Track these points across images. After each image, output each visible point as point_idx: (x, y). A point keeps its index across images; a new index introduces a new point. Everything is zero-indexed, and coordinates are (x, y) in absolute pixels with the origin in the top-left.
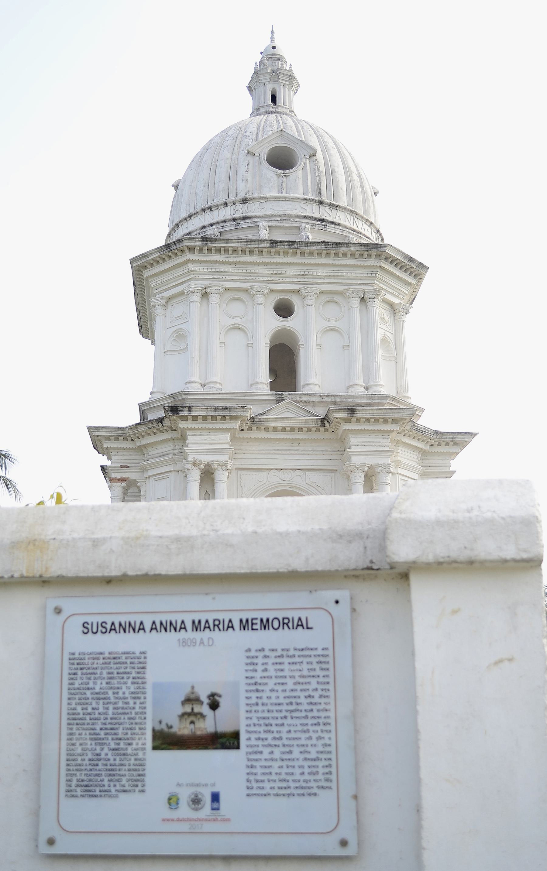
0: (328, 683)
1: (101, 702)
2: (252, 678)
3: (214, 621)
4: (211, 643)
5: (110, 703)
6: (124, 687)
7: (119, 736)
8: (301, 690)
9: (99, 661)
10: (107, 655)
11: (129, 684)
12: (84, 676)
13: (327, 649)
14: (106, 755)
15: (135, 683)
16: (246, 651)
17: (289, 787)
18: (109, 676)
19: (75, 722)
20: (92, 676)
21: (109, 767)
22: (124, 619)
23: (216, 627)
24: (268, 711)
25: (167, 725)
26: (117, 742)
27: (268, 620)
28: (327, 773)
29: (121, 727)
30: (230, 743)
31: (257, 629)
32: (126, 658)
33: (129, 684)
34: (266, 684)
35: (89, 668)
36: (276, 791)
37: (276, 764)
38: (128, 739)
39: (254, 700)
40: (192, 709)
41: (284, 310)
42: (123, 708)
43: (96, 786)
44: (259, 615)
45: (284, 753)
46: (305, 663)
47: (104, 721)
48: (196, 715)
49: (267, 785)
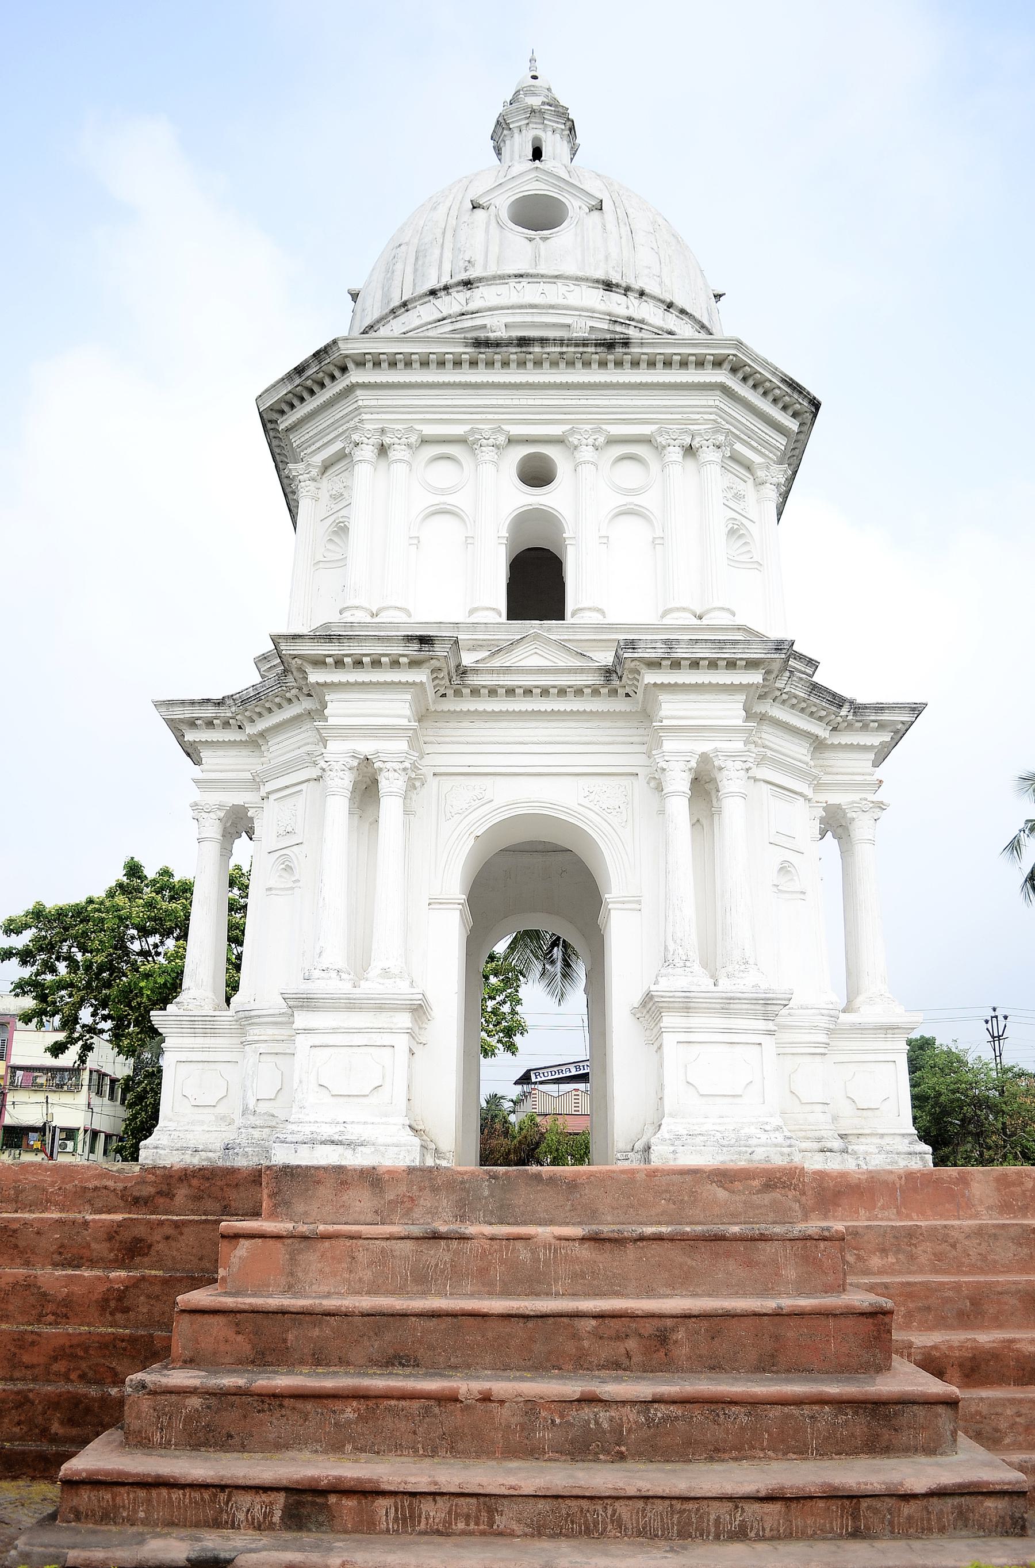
41: (537, 475)
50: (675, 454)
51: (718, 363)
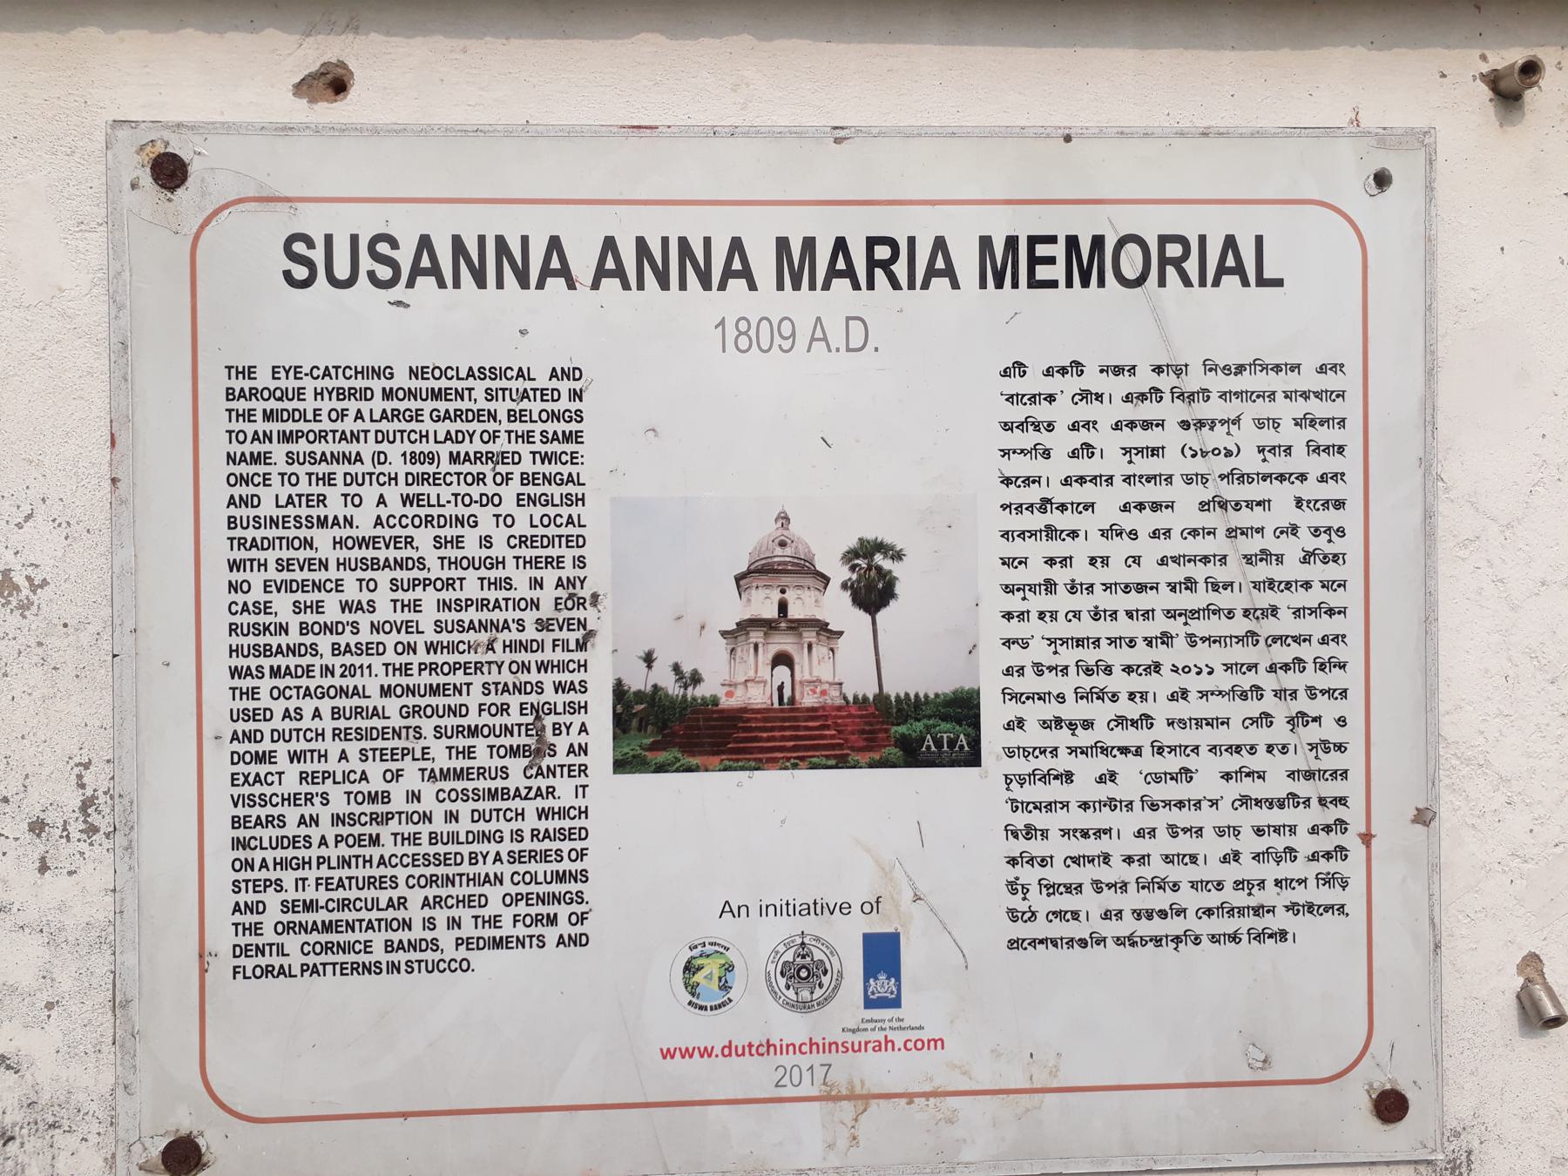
0: (1339, 504)
1: (384, 577)
2: (1029, 481)
3: (872, 242)
4: (856, 342)
5: (426, 583)
6: (485, 515)
7: (473, 719)
8: (1231, 533)
9: (365, 407)
10: (402, 380)
11: (509, 506)
12: (301, 470)
13: (1337, 367)
14: (415, 796)
15: (532, 500)
16: (1006, 373)
17: (1181, 912)
18: (417, 469)
19: (266, 663)
20: (340, 470)
21: (425, 848)
22: (473, 225)
23: (879, 273)
24: (1096, 615)
25: (676, 668)
26: (461, 742)
27: (1098, 242)
28: (1328, 855)
29: (477, 680)
30: (938, 743)
31: (1053, 284)
32: (490, 395)
33: (509, 506)
34: (1090, 506)
35: (322, 436)
36: (1127, 926)
37: (1125, 822)
38: (508, 730)
39: (1036, 572)
40: (783, 607)
42: (483, 604)
43: (370, 926)
44: (1060, 223)
45: (1157, 778)
46: (1246, 422)
47: (398, 660)
48: (797, 626)
49: (1088, 902)
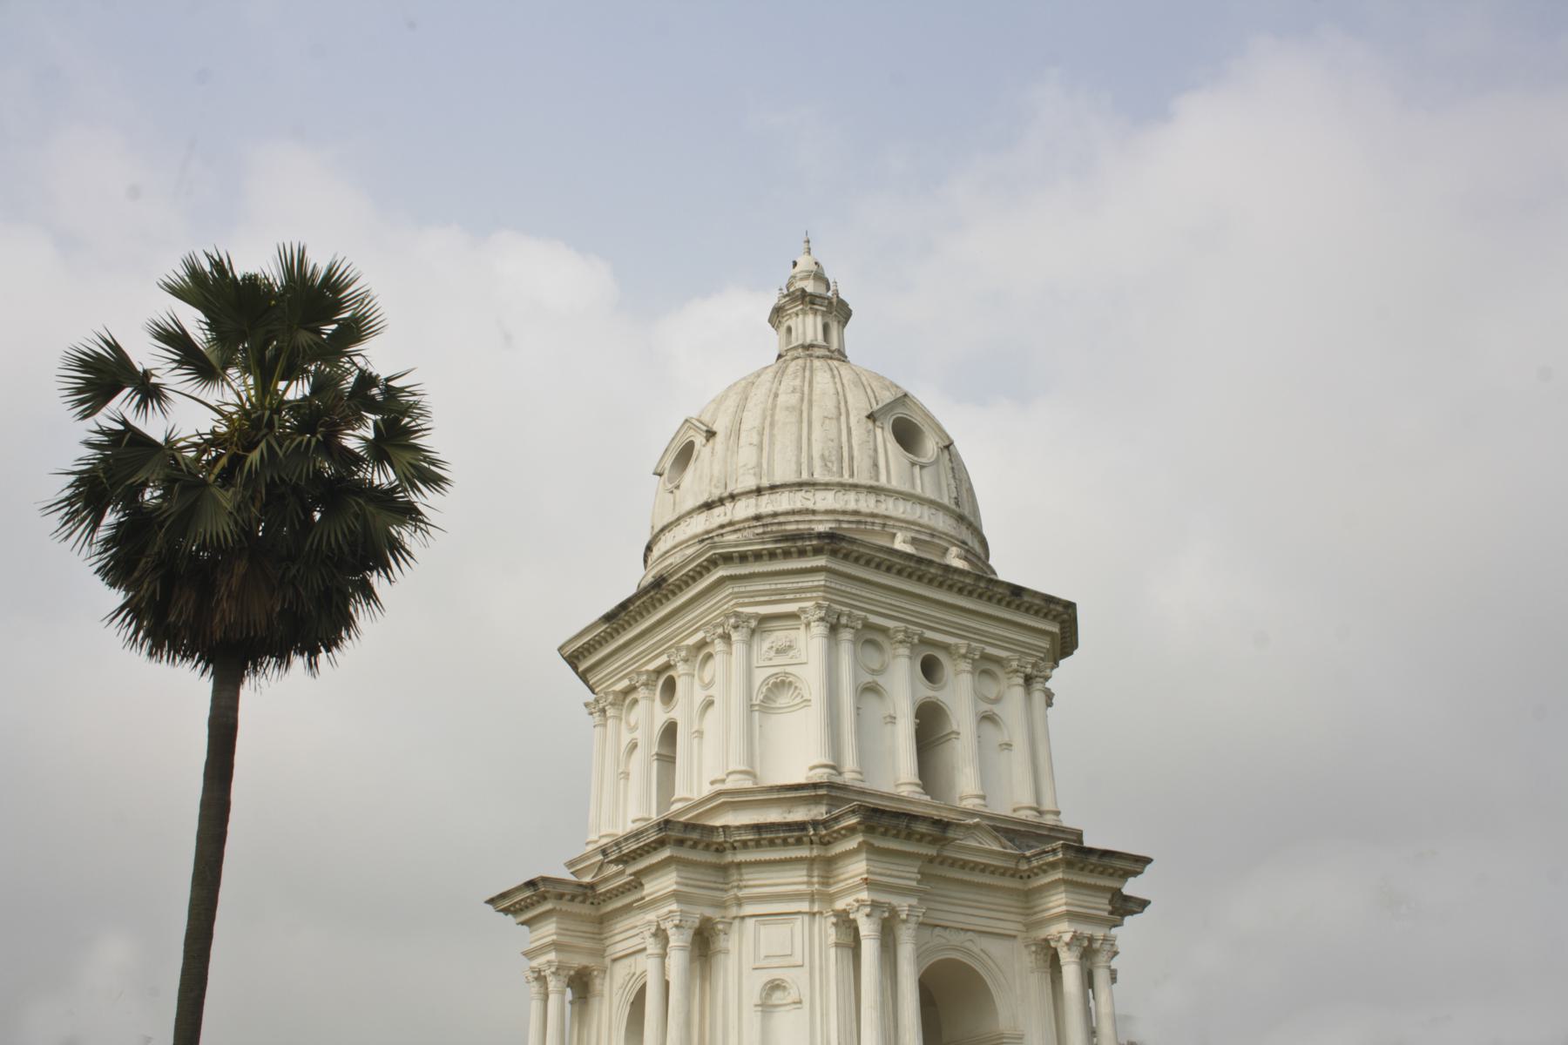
50: (719, 646)
51: (713, 563)
